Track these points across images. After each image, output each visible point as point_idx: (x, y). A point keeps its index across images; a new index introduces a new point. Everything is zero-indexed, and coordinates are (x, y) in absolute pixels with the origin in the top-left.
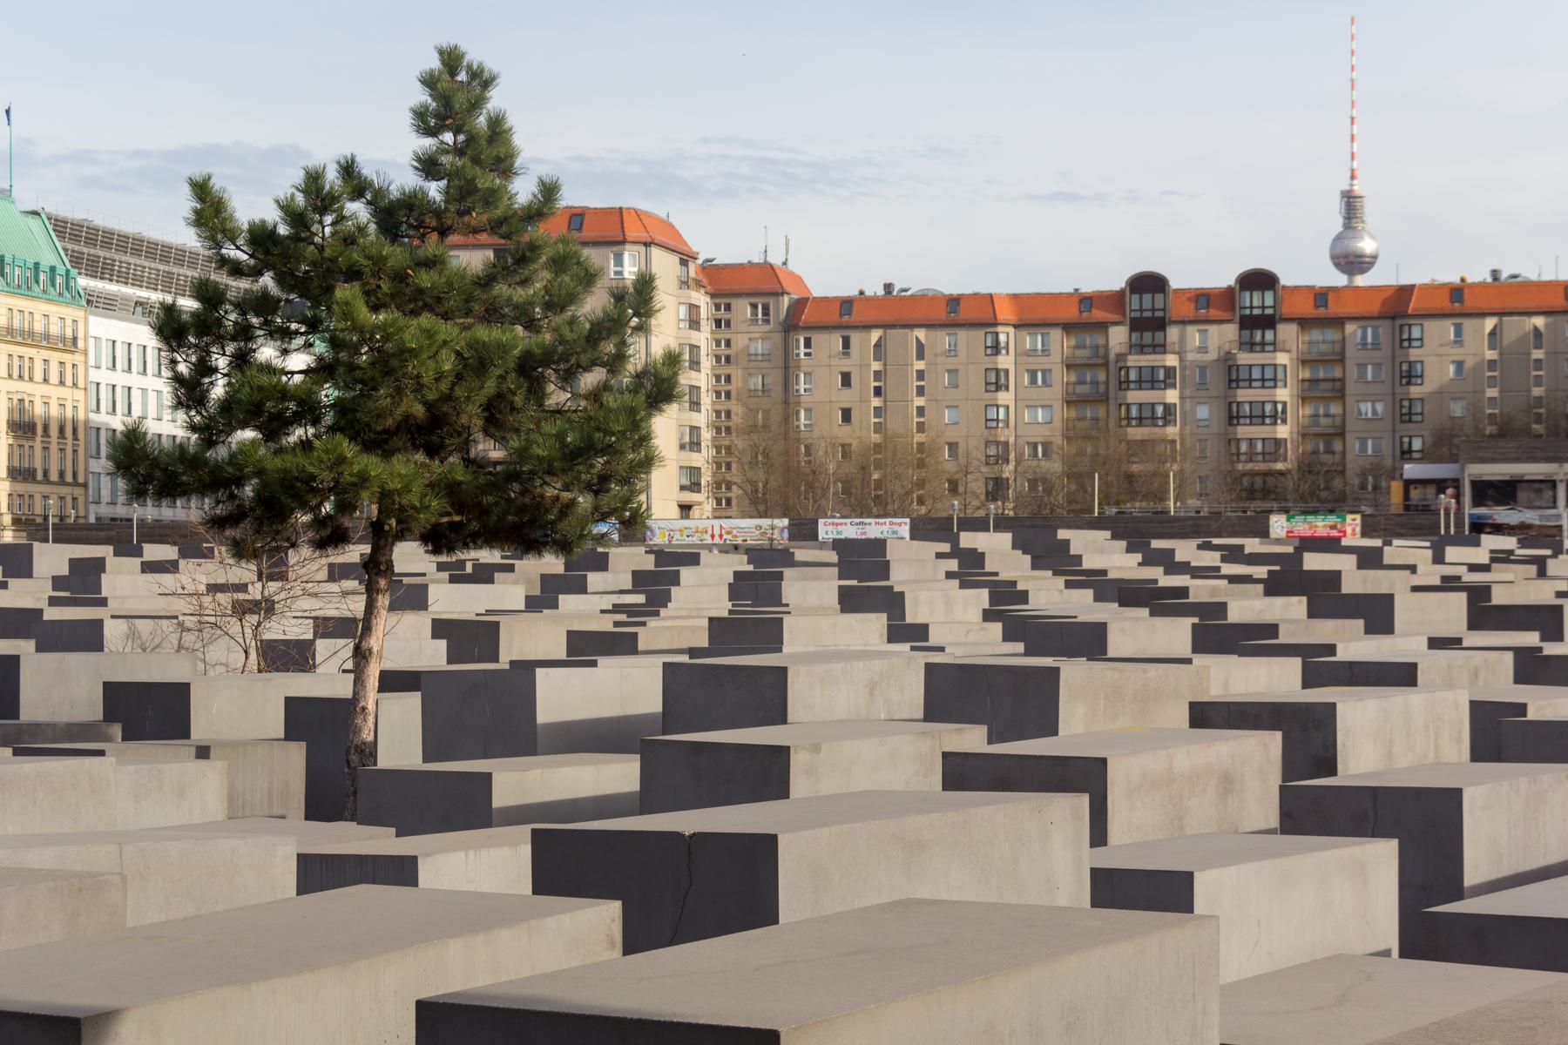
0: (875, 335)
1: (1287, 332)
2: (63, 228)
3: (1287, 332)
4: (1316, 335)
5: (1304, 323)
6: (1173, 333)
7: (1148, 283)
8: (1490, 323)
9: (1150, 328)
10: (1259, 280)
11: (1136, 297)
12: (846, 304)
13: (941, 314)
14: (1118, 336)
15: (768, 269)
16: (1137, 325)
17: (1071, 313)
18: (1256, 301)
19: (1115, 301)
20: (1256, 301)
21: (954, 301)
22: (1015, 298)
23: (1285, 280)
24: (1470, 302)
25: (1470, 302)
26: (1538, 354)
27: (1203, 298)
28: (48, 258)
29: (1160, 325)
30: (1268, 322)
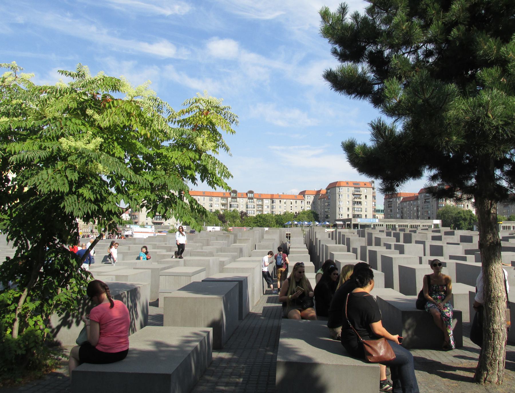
1: (255, 200)
3: (255, 200)
5: (258, 199)
6: (238, 199)
8: (285, 200)
10: (251, 192)
11: (232, 194)
13: (202, 194)
14: (230, 199)
16: (233, 198)
17: (222, 196)
18: (250, 195)
20: (250, 195)
21: (204, 192)
23: (255, 192)
27: (242, 194)
29: (236, 198)
30: (252, 198)
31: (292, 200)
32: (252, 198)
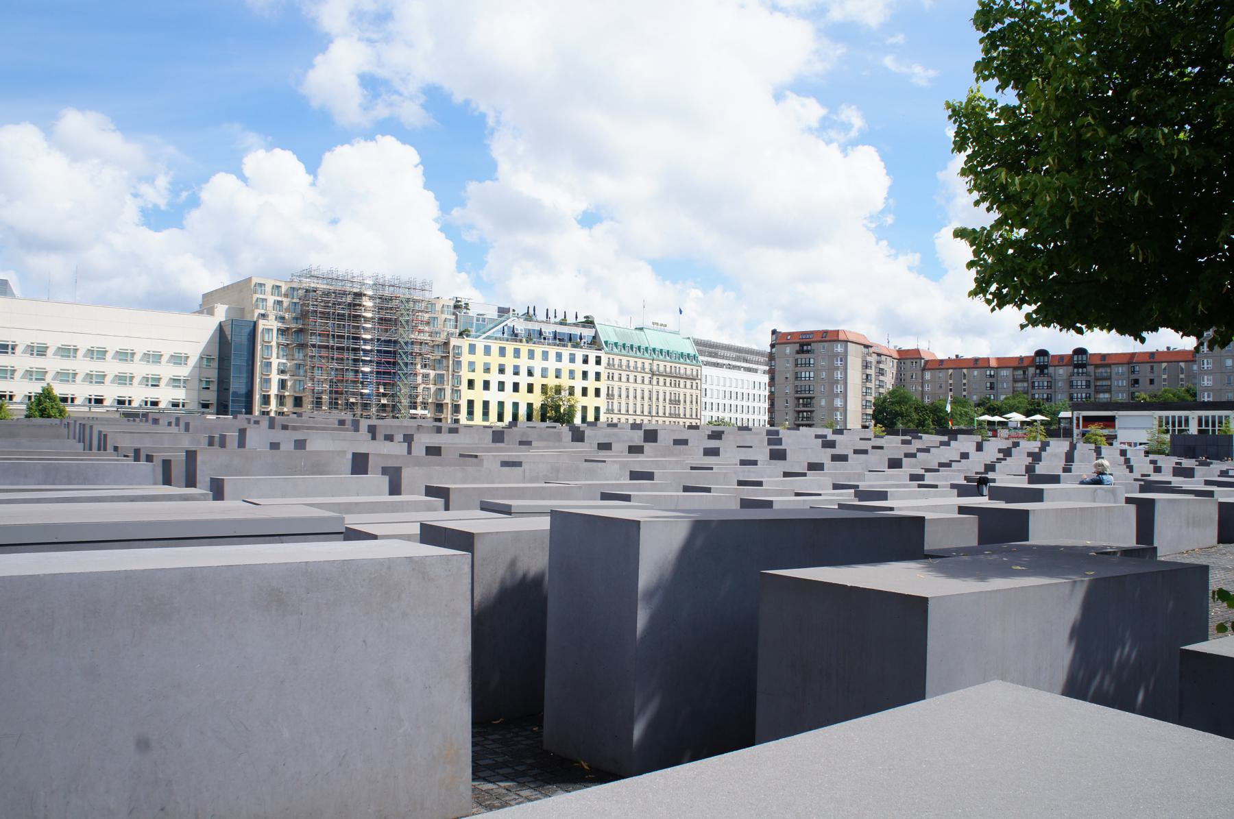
0: (951, 371)
2: (698, 343)
3: (1090, 369)
4: (1100, 370)
5: (1097, 366)
6: (1051, 369)
7: (1042, 353)
9: (1042, 368)
12: (942, 361)
15: (917, 351)
16: (1037, 367)
17: (1016, 364)
19: (1033, 358)
22: (998, 359)
24: (1157, 358)
25: (1157, 358)
26: (1182, 376)
27: (1061, 357)
28: (692, 353)
29: (1046, 367)
30: (1083, 366)
31: (1182, 364)
32: (1083, 366)
